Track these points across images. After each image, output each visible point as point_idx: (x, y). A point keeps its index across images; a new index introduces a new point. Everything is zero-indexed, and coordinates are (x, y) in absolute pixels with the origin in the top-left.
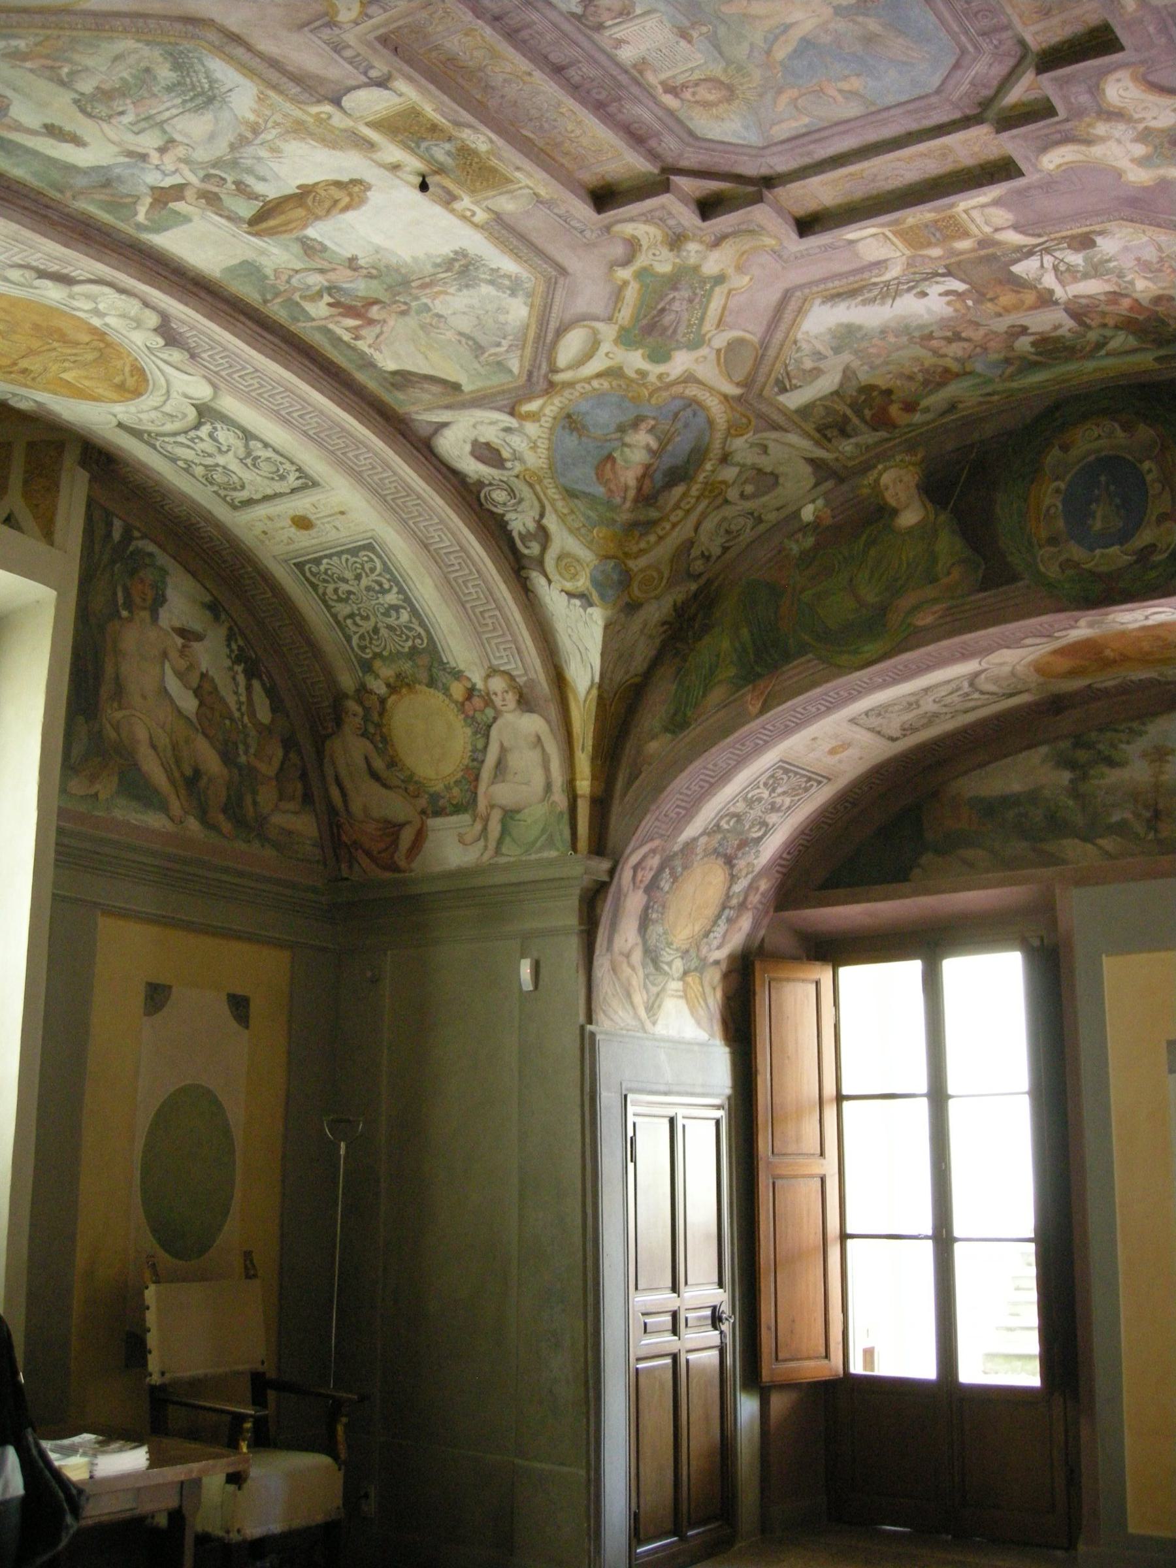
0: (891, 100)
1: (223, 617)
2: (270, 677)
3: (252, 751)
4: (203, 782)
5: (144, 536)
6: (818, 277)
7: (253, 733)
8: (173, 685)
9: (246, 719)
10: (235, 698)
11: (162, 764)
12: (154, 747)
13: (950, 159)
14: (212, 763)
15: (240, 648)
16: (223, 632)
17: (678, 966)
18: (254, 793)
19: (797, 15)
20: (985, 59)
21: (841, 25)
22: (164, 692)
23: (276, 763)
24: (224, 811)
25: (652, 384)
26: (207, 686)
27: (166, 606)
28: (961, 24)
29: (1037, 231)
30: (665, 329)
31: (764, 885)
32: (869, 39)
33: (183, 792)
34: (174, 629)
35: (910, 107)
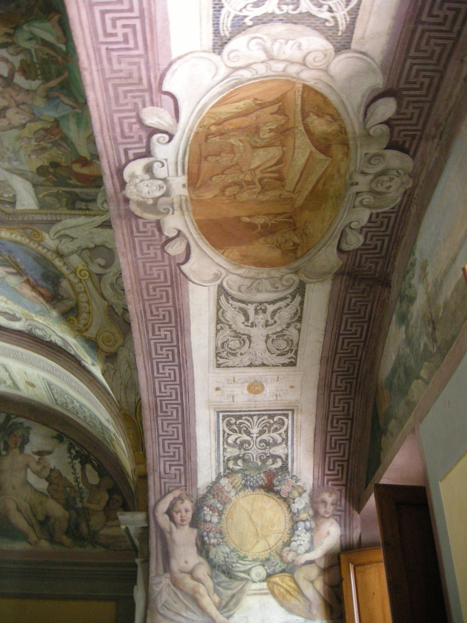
1: (65, 439)
2: (97, 460)
3: (85, 500)
4: (52, 520)
5: (17, 416)
7: (86, 490)
8: (32, 478)
9: (81, 485)
10: (74, 476)
11: (25, 518)
12: (19, 510)
14: (56, 509)
15: (77, 452)
16: (64, 447)
17: (259, 572)
18: (88, 521)
22: (27, 483)
23: (103, 504)
24: (67, 533)
26: (54, 474)
27: (29, 444)
31: (329, 498)
33: (38, 528)
34: (34, 453)
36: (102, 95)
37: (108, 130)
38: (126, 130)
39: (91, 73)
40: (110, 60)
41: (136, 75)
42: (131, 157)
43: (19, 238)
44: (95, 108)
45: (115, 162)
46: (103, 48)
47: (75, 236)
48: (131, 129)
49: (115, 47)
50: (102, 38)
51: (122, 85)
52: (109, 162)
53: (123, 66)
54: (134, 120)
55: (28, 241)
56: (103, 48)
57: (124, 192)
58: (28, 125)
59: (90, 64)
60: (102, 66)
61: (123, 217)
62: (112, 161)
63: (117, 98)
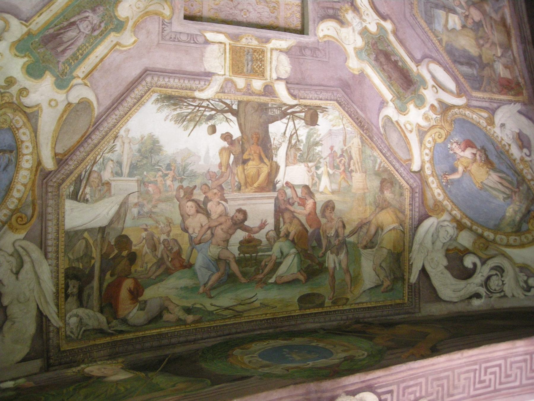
6: (170, 67)
25: (12, 96)
29: (296, 92)
30: (61, 44)
36: (442, 368)
37: (412, 375)
38: (410, 390)
39: (459, 359)
40: (468, 372)
41: (456, 391)
42: (383, 397)
43: (16, 194)
44: (432, 363)
45: (379, 382)
46: (477, 367)
47: (20, 277)
48: (411, 393)
49: (477, 375)
50: (484, 366)
51: (448, 382)
52: (379, 377)
53: (462, 382)
54: (418, 395)
55: (12, 207)
56: (477, 367)
57: (343, 394)
58: (187, 234)
59: (465, 357)
60: (464, 366)
61: (307, 397)
62: (380, 380)
63: (438, 379)
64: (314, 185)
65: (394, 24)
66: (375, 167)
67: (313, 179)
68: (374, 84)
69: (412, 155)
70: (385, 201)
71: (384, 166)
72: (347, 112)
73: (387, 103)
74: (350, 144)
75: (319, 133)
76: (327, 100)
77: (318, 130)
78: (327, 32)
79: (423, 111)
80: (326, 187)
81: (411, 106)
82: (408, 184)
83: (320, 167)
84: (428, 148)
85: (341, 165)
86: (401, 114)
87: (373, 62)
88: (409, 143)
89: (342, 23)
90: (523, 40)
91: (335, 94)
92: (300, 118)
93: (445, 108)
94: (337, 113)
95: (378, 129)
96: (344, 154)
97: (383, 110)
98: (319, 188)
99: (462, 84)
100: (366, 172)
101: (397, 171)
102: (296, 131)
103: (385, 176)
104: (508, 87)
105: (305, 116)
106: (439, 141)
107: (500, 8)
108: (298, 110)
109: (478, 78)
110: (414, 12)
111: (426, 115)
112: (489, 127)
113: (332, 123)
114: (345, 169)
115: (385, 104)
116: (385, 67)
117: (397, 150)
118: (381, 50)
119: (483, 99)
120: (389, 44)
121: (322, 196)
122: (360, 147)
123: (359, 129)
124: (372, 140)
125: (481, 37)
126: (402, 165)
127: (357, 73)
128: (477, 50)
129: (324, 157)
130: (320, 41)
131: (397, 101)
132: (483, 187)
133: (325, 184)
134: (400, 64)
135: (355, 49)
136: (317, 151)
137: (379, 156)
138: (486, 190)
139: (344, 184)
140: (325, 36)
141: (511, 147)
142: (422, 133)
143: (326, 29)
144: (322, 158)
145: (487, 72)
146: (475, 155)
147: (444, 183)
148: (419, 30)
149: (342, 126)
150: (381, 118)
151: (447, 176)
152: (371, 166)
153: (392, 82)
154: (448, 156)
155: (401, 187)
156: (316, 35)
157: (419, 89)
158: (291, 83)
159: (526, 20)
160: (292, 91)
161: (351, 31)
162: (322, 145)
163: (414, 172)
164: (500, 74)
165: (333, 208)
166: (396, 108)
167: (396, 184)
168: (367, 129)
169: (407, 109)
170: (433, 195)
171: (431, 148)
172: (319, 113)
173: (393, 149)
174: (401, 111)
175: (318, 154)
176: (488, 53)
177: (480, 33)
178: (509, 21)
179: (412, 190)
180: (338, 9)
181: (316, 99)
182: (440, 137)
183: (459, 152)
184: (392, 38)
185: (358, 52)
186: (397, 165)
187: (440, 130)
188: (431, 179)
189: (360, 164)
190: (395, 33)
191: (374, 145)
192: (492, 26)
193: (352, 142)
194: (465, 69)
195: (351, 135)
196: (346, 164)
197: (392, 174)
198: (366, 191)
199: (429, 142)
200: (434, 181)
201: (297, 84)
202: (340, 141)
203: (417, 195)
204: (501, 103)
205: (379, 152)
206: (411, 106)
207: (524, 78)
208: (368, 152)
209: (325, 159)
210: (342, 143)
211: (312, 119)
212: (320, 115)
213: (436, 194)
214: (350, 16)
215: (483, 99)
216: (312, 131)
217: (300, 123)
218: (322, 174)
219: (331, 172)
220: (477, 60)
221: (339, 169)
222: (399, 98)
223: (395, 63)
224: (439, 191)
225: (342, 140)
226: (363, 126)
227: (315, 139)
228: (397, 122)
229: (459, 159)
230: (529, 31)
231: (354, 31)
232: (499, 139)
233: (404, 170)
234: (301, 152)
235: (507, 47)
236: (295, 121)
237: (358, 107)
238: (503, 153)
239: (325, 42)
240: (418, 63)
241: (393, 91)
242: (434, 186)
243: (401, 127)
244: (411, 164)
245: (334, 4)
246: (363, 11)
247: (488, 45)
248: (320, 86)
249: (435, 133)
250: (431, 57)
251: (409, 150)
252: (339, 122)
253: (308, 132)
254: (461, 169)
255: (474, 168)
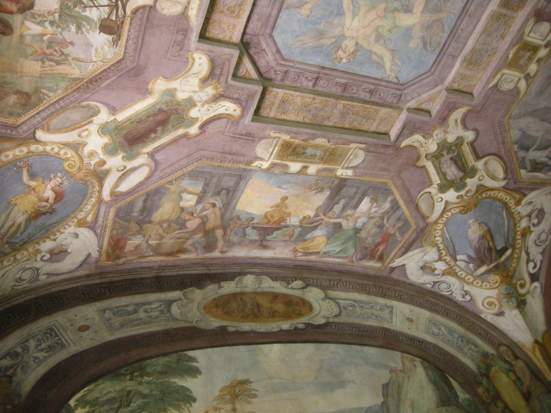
0: (284, 15)
13: (226, 11)
19: (355, 23)
20: (273, 63)
21: (337, 31)
28: (298, 68)
29: (139, 15)
32: (321, 35)
35: (272, 19)
64: (33, 16)
65: (194, 137)
66: (45, 89)
67: (39, 16)
68: (135, 104)
69: (53, 133)
70: (6, 94)
71: (45, 99)
72: (109, 68)
73: (113, 115)
74: (73, 65)
75: (91, 32)
76: (126, 48)
77: (94, 32)
78: (197, 62)
79: (100, 152)
80: (29, 29)
81: (106, 140)
82: (22, 123)
83: (52, 27)
84: (59, 151)
85: (52, 51)
86: (100, 127)
87: (158, 107)
88: (66, 131)
89: (205, 81)
90: (162, 268)
91: (130, 58)
92: (110, 14)
93: (100, 176)
94: (109, 56)
95: (87, 99)
96: (63, 56)
97: (106, 109)
98: (29, 20)
99: (124, 199)
100: (40, 77)
101: (38, 113)
102: (97, 7)
103: (34, 99)
104: (117, 246)
105: (112, 20)
106: (66, 164)
107: (196, 249)
108: (120, 13)
109: (128, 217)
110: (204, 160)
111: (95, 155)
112: (76, 220)
113: (100, 48)
114: (47, 55)
115: (112, 112)
116: (151, 118)
117: (61, 117)
118: (169, 117)
119: (106, 219)
120: (175, 127)
121: (19, 22)
122: (69, 76)
123: (88, 78)
124: (74, 91)
125: (169, 226)
126: (44, 119)
127: (150, 86)
128: (157, 220)
129: (63, 33)
130: (190, 53)
131: (113, 126)
132: (10, 206)
133: (33, 28)
134: (153, 135)
135: (175, 90)
136: (71, 26)
137: (56, 95)
138: (7, 208)
139: (30, 51)
140: (194, 60)
141: (53, 242)
142: (77, 147)
143: (201, 63)
144: (63, 31)
145: (134, 226)
146: (47, 201)
147: (19, 164)
148: (184, 162)
149: (95, 59)
150: (98, 104)
151: (26, 168)
152: (47, 85)
153: (135, 124)
154: (49, 172)
155: (20, 115)
156: (196, 50)
157: (124, 151)
158: (149, 11)
159: (181, 273)
160: (141, 11)
161: (194, 89)
162: (77, 33)
163: (34, 133)
164: (130, 240)
165: (4, 34)
166: (107, 123)
167: (23, 109)
168: (87, 87)
169: (104, 135)
170: (7, 150)
171: (59, 155)
172: (112, 36)
173: (62, 112)
174: (103, 128)
175: (68, 27)
176: (153, 231)
177: (174, 225)
178: (183, 256)
179: (15, 127)
180: (219, 80)
181: (128, 36)
182: (70, 166)
183: (52, 184)
184: (181, 132)
185: (171, 92)
186: (44, 114)
187: (78, 166)
188: (25, 149)
189: (50, 72)
190: (185, 136)
191: (69, 92)
192: (179, 238)
193: (75, 67)
194: (139, 204)
195: (84, 69)
196: (52, 57)
197: (35, 107)
198: (19, 74)
199: (66, 154)
200: (23, 153)
201: (148, 18)
202: (78, 54)
203: (9, 132)
204: (100, 237)
205: (62, 96)
206: (106, 140)
207: (124, 264)
208: (63, 84)
209: (61, 33)
210: (76, 56)
211: (106, 27)
212: (110, 38)
213: (8, 153)
214: (210, 91)
215: (106, 219)
216: (94, 25)
217: (104, 12)
218: (44, 26)
219: (45, 38)
220: (147, 219)
221: (47, 48)
222: (117, 128)
223: (154, 131)
224: (11, 157)
225: (79, 57)
226: (91, 83)
227: (84, 27)
228: (92, 122)
229: (44, 183)
230: (170, 274)
231: (195, 92)
232: (62, 230)
233: (38, 121)
234: (72, 7)
235: (157, 250)
236: (107, 8)
237: (113, 81)
238: (47, 232)
239: (188, 59)
240: (151, 155)
241: (125, 122)
242: (17, 152)
243: (85, 125)
244: (44, 130)
245: (225, 77)
246: (213, 106)
247: (161, 231)
248: (142, 43)
249: (74, 161)
250: (155, 170)
251: (59, 130)
252: (99, 57)
253: (93, 20)
254: (33, 183)
255: (33, 198)
